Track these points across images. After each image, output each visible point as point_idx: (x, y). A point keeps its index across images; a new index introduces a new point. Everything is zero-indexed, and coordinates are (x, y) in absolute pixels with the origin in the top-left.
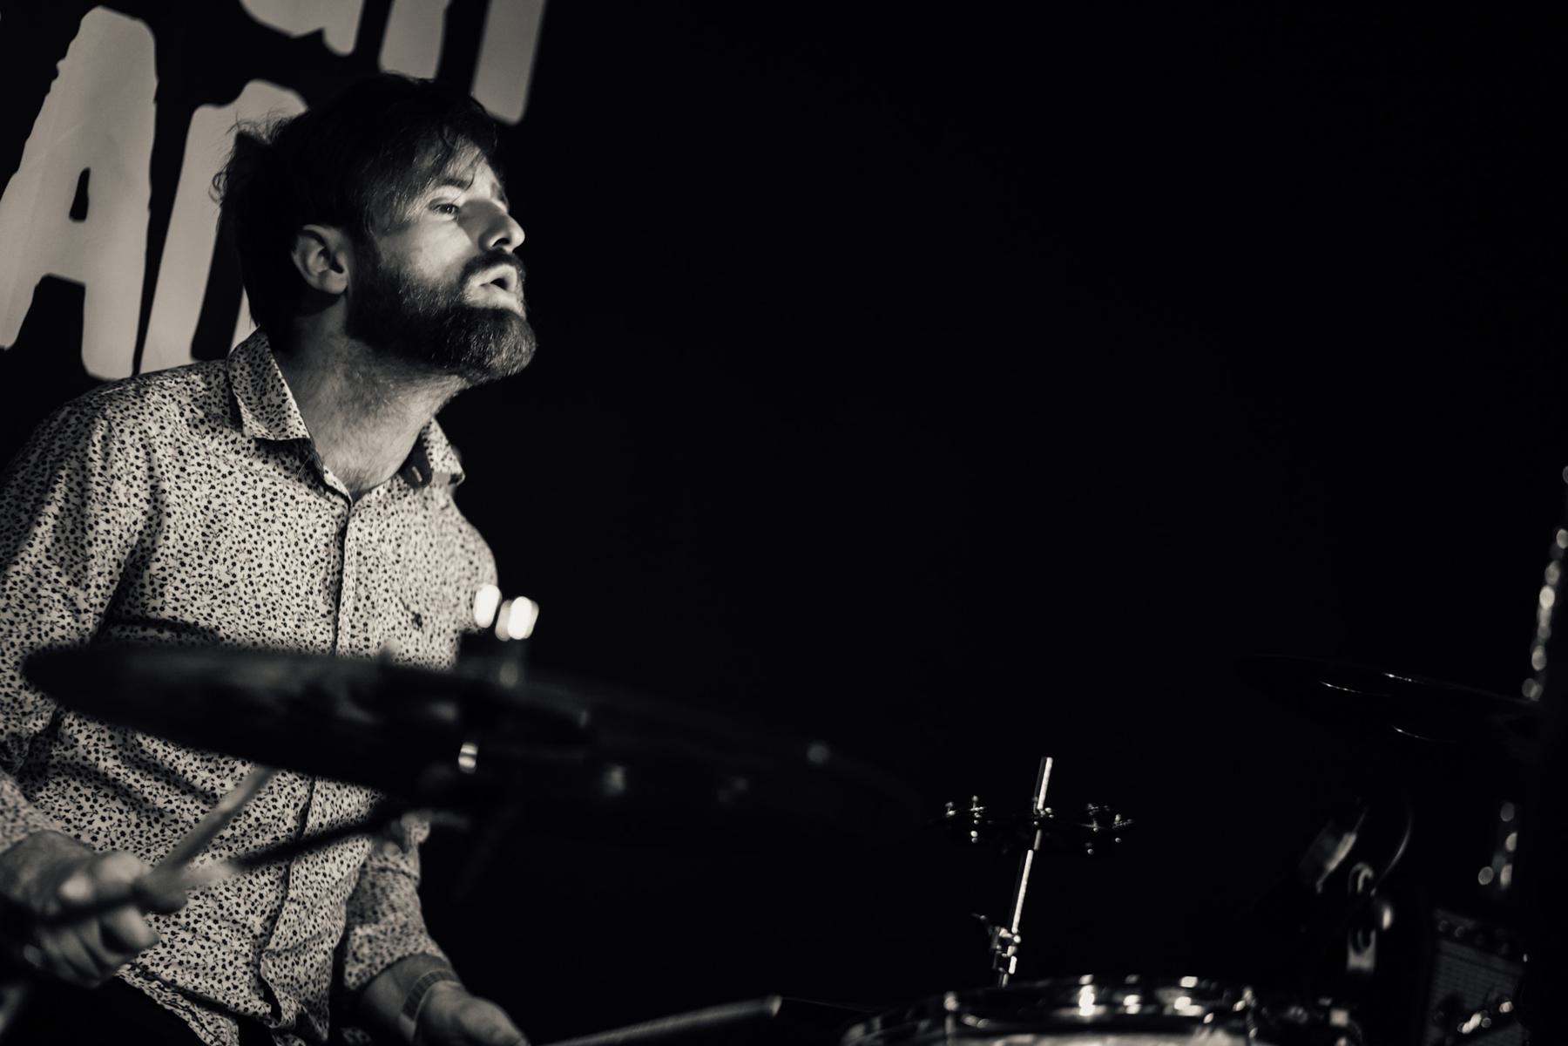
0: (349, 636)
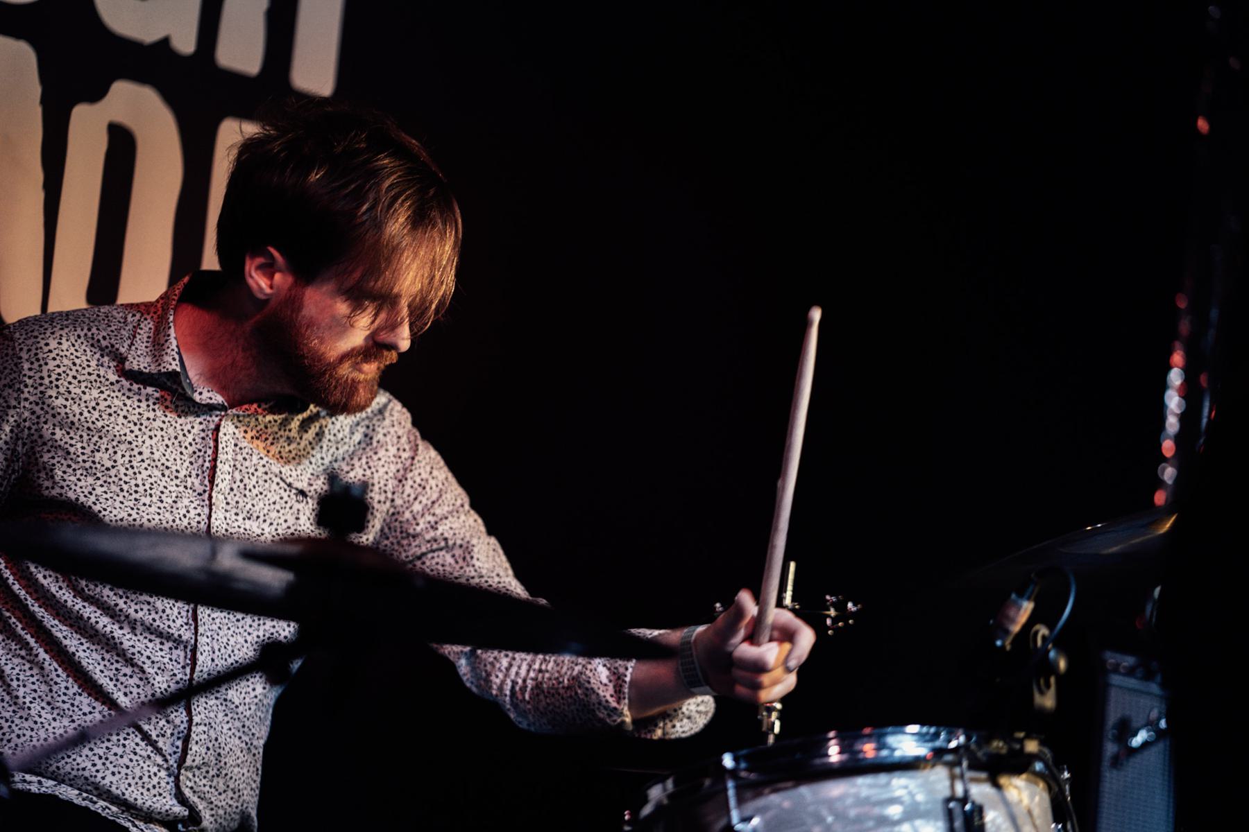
0: (223, 511)
